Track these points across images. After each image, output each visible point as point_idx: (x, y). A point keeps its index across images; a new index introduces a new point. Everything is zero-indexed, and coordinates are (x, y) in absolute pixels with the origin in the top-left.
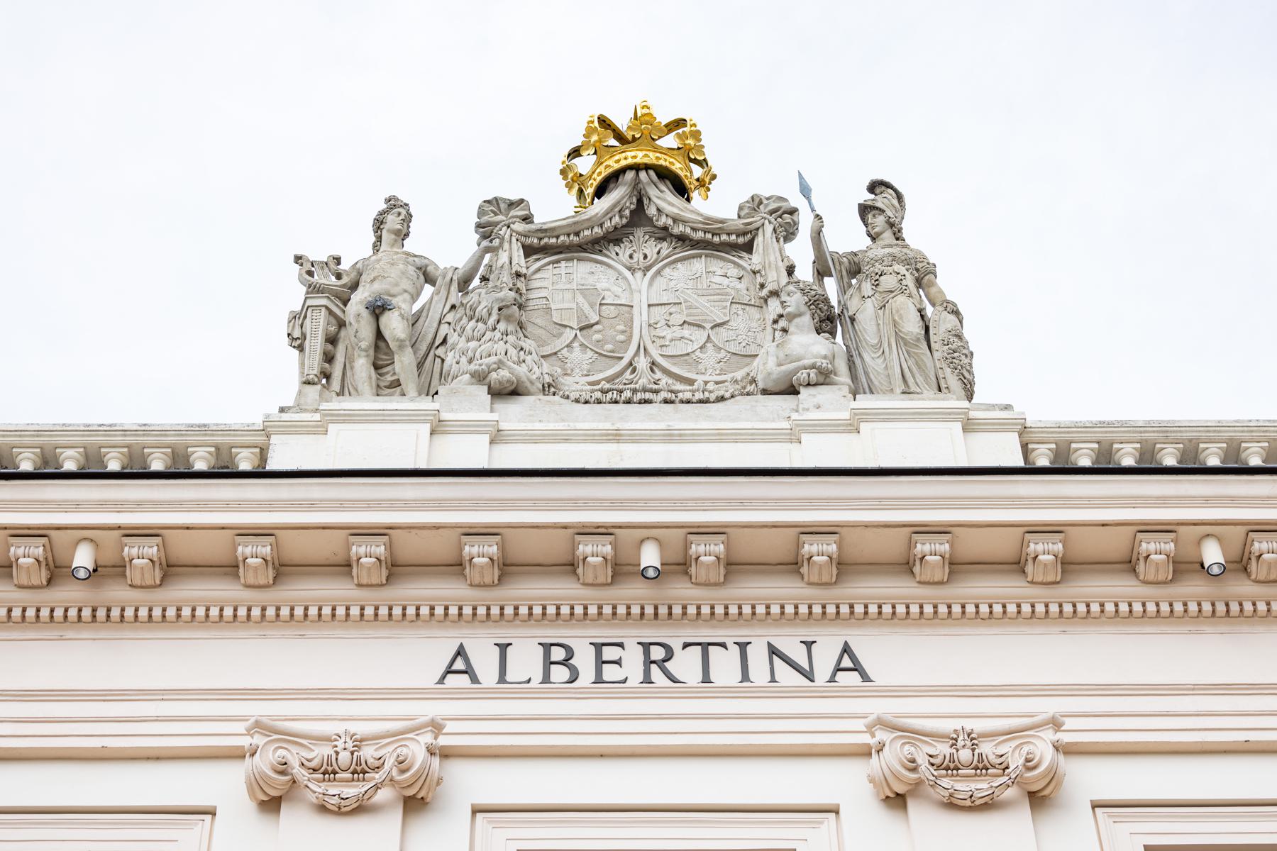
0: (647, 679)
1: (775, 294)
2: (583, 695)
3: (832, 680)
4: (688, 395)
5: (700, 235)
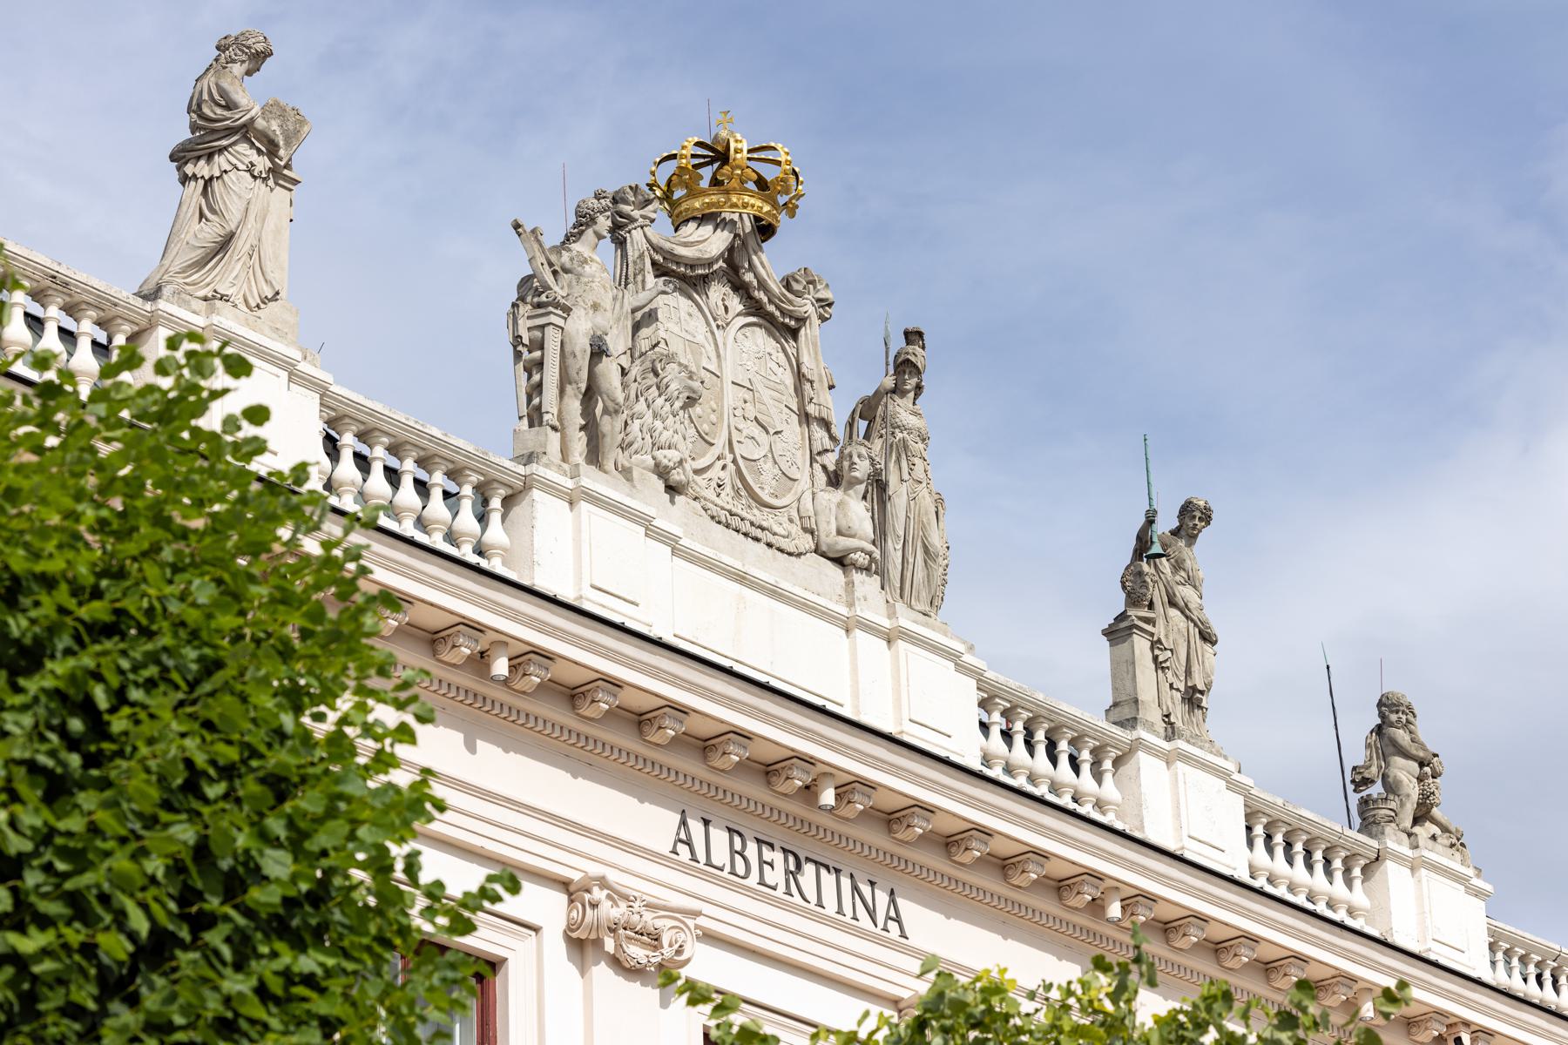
5: (771, 308)
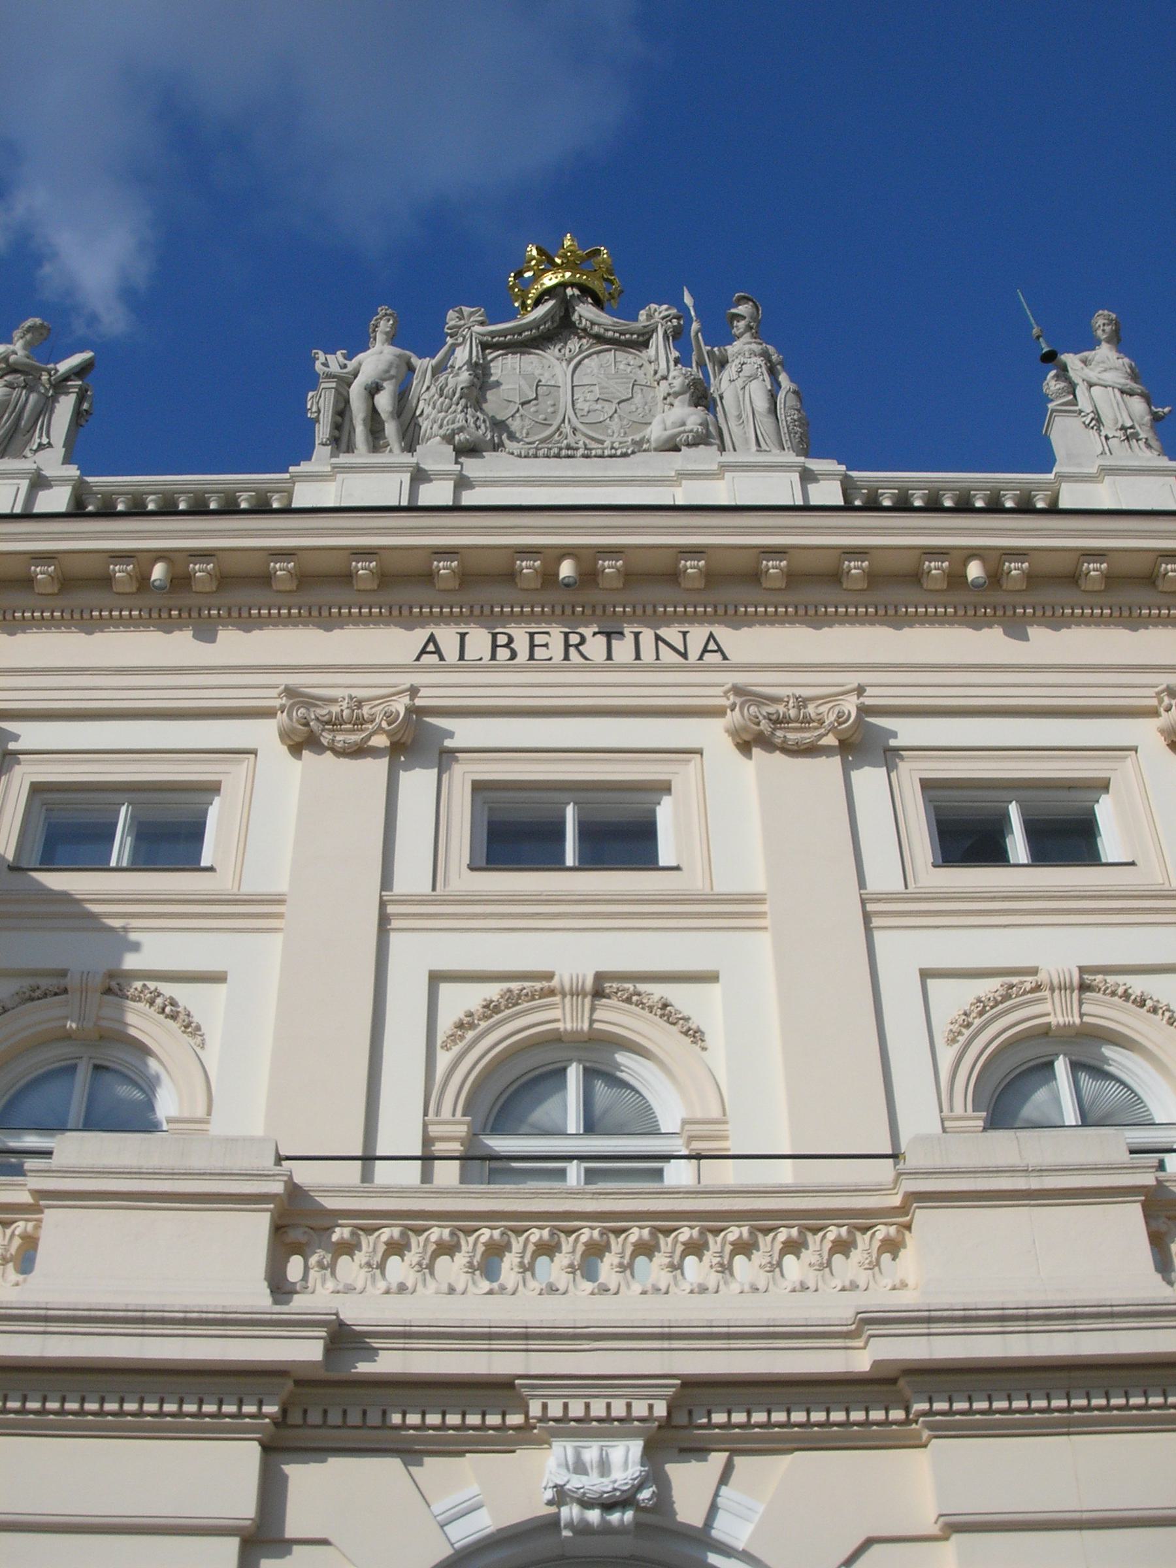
0: (567, 658)
1: (665, 378)
2: (521, 669)
3: (701, 658)
4: (599, 452)
5: (610, 334)
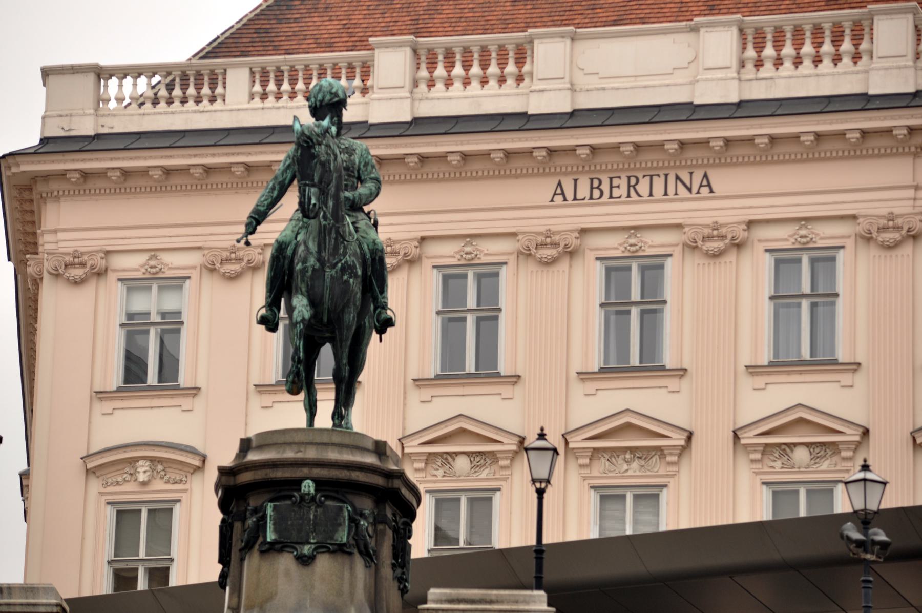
0: (629, 196)
3: (698, 193)
